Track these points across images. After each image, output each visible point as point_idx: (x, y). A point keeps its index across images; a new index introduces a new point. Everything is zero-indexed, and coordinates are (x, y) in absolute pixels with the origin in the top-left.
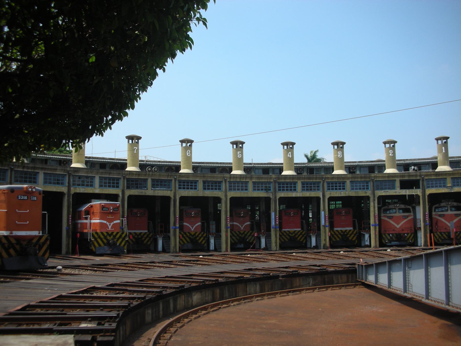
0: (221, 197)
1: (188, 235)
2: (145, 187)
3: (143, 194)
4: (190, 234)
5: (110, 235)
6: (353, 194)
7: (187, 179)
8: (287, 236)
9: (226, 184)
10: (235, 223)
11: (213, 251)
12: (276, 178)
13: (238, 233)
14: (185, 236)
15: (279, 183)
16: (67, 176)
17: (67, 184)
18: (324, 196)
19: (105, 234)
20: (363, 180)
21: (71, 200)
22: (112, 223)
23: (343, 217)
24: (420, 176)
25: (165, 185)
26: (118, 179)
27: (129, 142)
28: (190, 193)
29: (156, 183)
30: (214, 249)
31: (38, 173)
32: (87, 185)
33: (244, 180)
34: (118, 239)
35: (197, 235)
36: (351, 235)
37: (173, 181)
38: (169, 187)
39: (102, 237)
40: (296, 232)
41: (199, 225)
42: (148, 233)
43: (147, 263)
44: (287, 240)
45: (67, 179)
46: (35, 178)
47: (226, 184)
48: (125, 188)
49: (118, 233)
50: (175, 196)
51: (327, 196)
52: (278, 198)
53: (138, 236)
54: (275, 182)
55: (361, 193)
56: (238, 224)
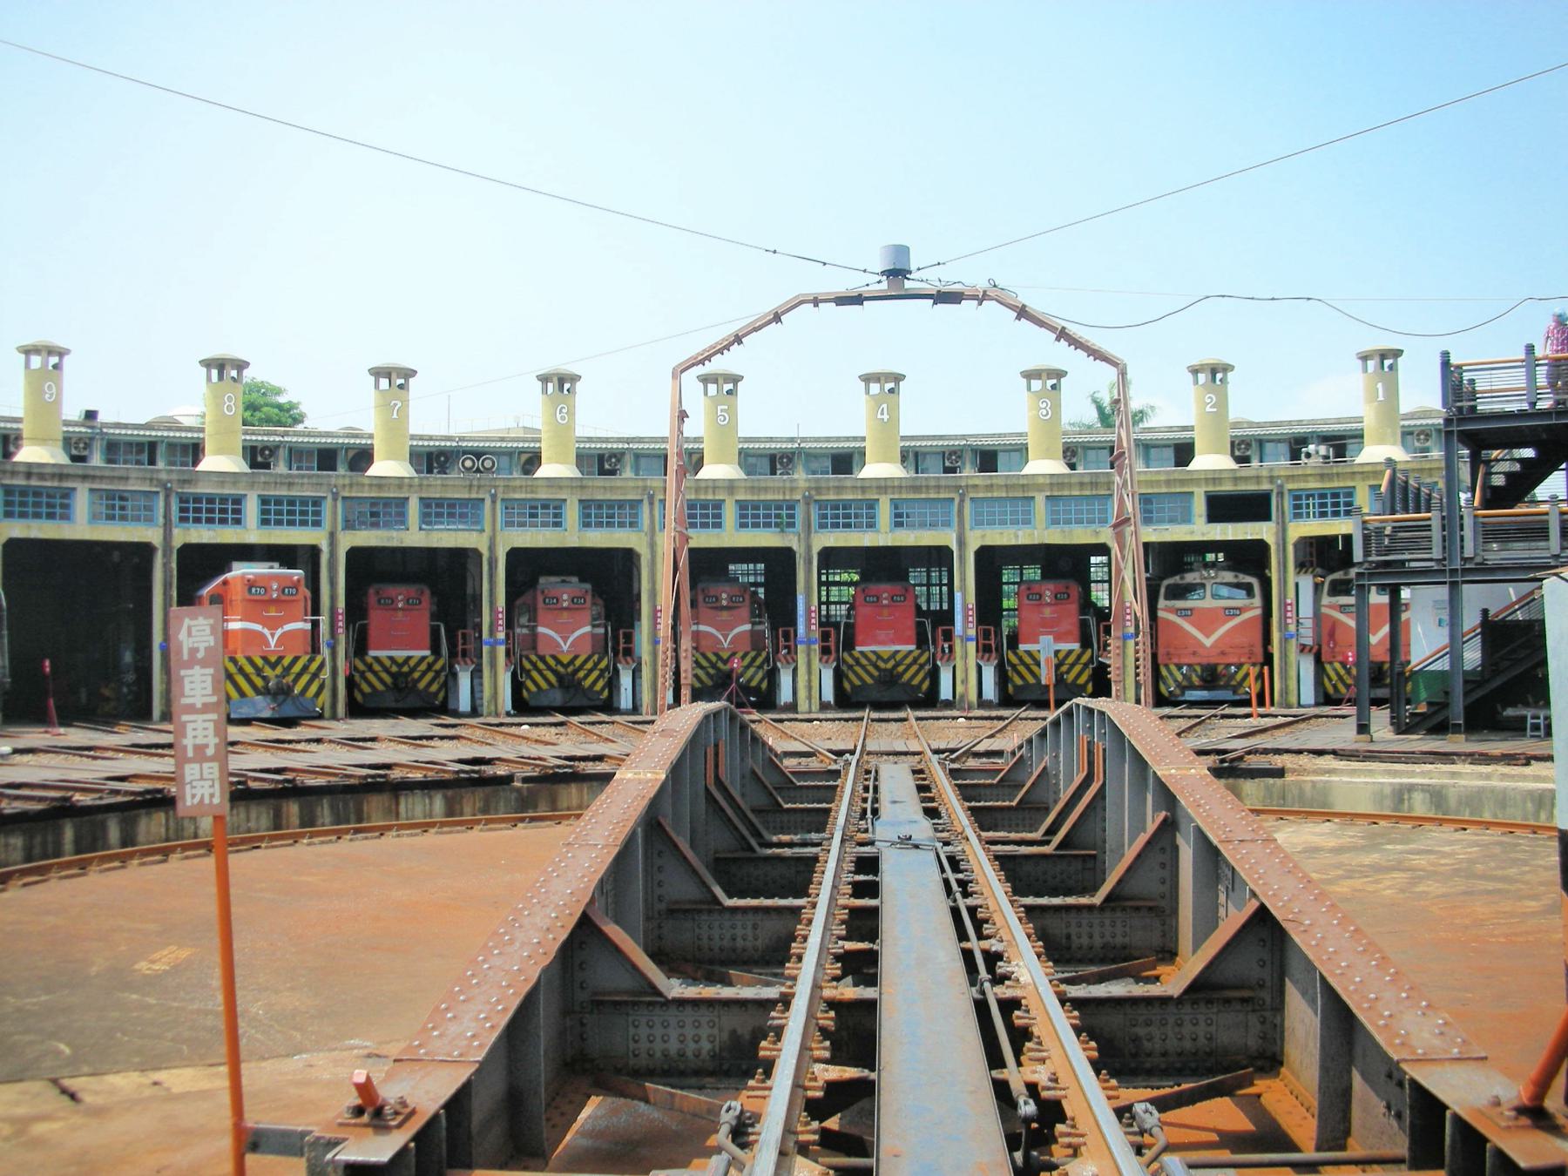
0: (638, 549)
1: (552, 662)
2: (403, 523)
3: (395, 544)
4: (558, 662)
5: (273, 666)
6: (1055, 536)
7: (529, 496)
8: (870, 668)
9: (651, 510)
10: (702, 628)
11: (627, 713)
12: (809, 489)
13: (714, 659)
14: (541, 665)
15: (822, 505)
16: (161, 497)
17: (161, 520)
18: (962, 543)
19: (260, 662)
20: (1088, 493)
21: (174, 565)
22: (279, 632)
23: (886, 612)
24: (1272, 479)
25: (463, 516)
26: (317, 502)
27: (377, 386)
28: (540, 537)
29: (434, 510)
30: (630, 706)
31: (74, 489)
32: (223, 521)
33: (710, 497)
34: (299, 675)
35: (578, 663)
36: (1073, 665)
37: (488, 503)
38: (478, 520)
39: (249, 669)
40: (898, 657)
41: (583, 636)
42: (431, 659)
43: (299, 742)
44: (869, 680)
45: (161, 504)
46: (66, 506)
47: (651, 510)
48: (340, 527)
49: (296, 659)
50: (492, 548)
51: (973, 545)
52: (816, 550)
53: (400, 666)
54: (808, 501)
55: (1081, 536)
56: (713, 631)
